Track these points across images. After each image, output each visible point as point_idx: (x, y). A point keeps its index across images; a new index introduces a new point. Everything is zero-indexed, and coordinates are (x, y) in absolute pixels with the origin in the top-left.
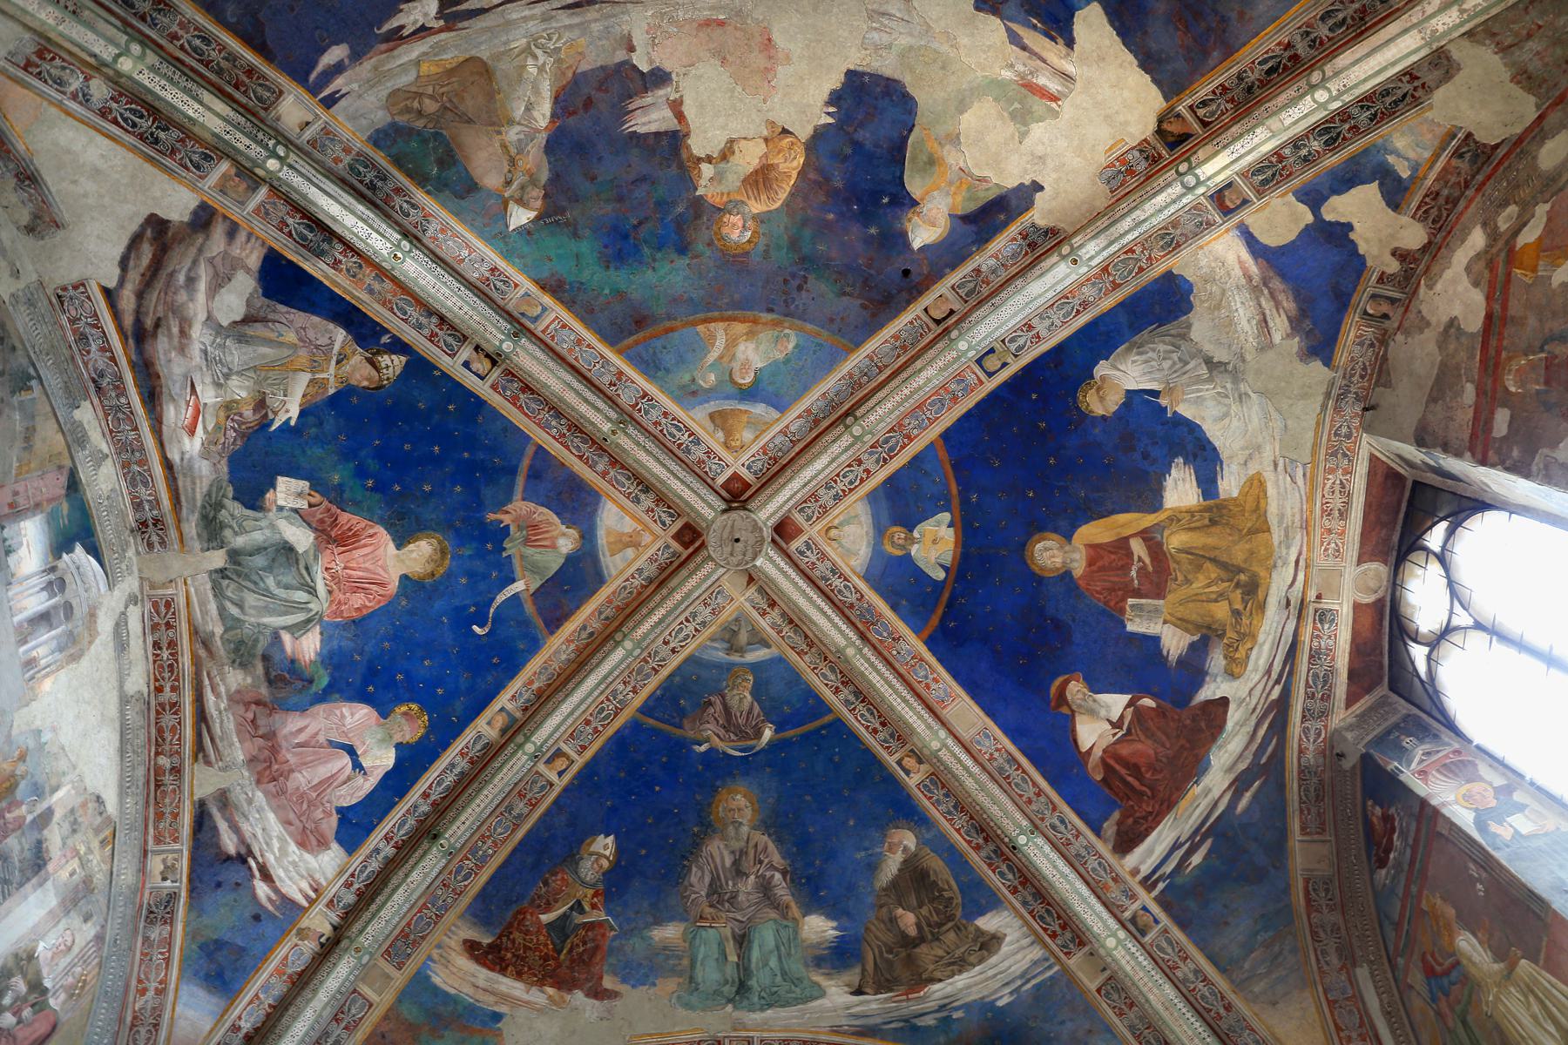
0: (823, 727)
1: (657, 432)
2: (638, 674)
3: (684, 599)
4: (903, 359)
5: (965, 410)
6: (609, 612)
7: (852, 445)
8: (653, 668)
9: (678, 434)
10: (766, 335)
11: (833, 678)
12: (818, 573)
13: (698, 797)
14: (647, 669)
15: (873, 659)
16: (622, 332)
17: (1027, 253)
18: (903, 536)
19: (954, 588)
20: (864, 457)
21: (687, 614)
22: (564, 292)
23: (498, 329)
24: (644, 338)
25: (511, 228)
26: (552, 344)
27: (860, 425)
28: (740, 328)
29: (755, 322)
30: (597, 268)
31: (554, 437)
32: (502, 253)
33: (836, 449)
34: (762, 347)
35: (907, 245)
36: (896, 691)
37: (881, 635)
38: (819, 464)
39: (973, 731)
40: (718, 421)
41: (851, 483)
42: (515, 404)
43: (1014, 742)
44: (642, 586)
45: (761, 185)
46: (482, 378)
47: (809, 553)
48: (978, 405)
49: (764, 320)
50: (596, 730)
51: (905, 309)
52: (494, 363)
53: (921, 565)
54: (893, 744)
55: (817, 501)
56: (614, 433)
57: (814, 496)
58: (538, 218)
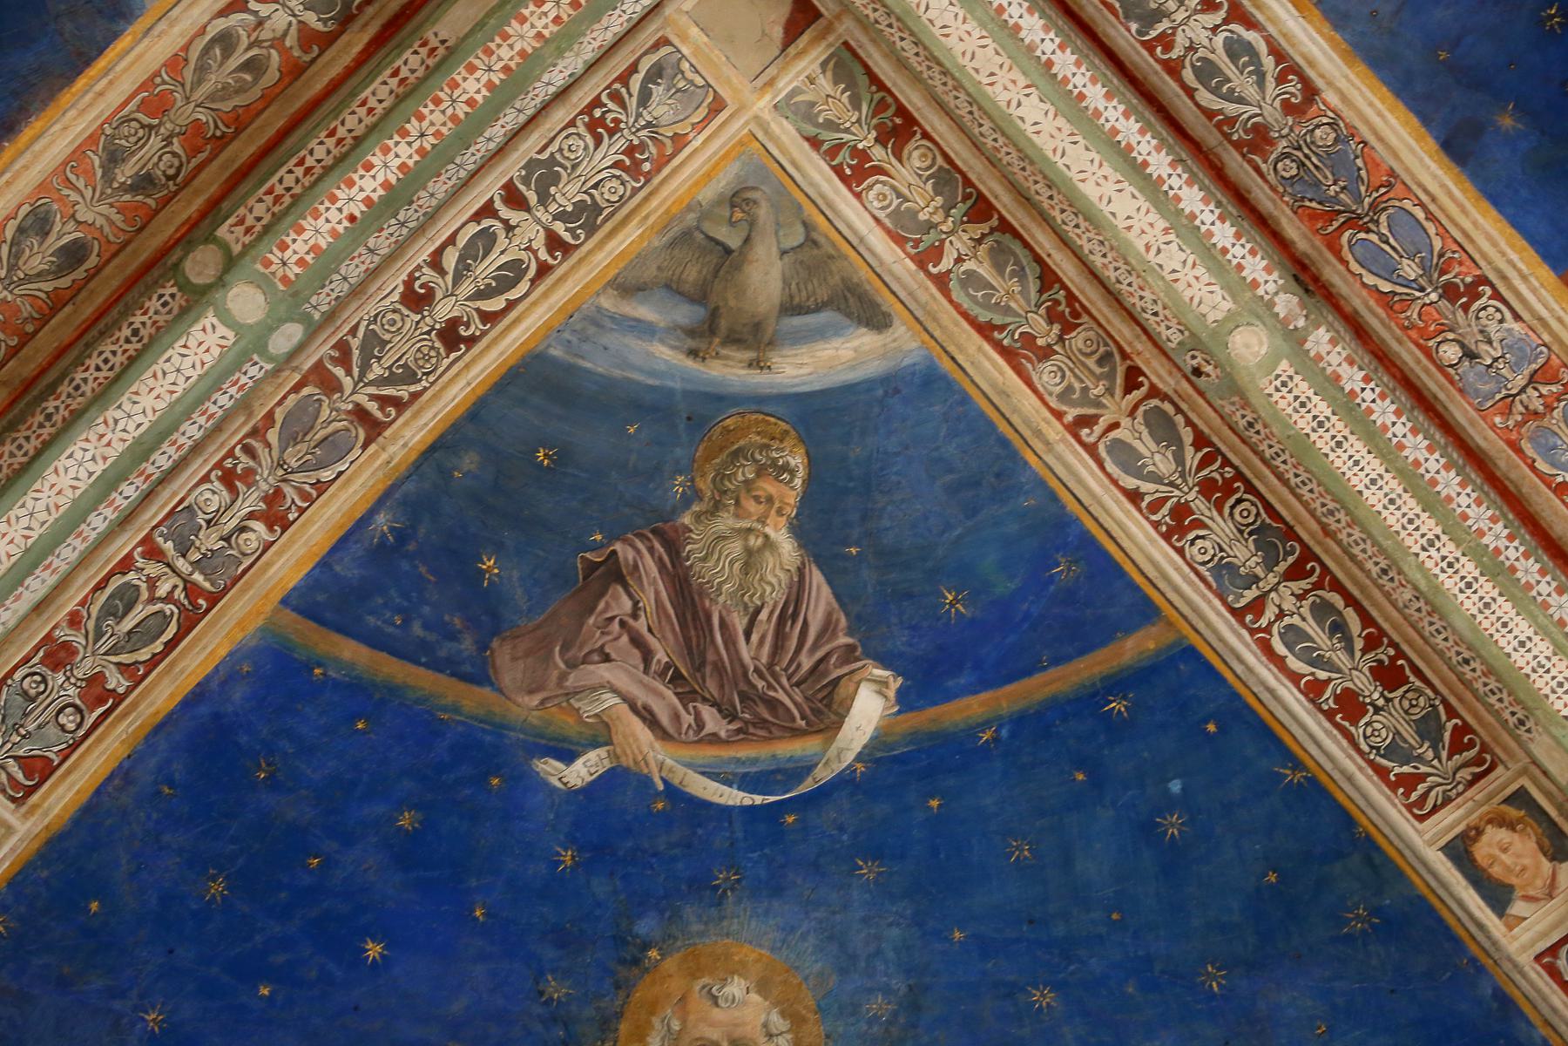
0: (1116, 684)
2: (289, 439)
3: (501, 96)
6: (151, 154)
8: (360, 414)
11: (1163, 464)
13: (556, 989)
14: (331, 416)
15: (1352, 378)
21: (511, 168)
36: (1454, 526)
44: (308, 37)
50: (96, 691)
54: (1436, 766)
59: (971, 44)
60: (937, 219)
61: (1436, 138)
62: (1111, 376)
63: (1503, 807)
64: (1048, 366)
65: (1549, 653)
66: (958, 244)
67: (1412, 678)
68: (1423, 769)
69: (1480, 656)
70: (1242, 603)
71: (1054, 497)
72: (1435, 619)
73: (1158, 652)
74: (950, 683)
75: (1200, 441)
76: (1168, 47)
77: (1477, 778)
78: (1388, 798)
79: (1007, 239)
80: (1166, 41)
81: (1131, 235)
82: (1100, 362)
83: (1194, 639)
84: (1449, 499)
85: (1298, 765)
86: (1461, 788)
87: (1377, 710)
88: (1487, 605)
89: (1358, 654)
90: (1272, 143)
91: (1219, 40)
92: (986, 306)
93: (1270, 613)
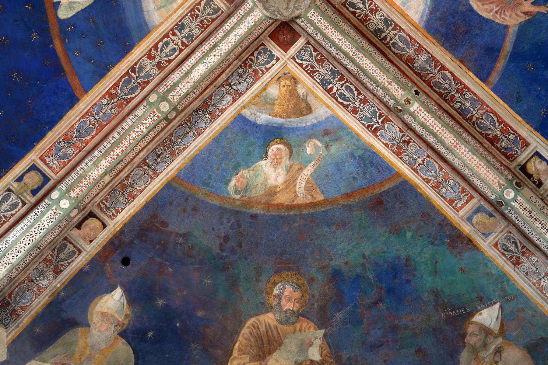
1: (364, 92)
4: (123, 175)
5: (56, 128)
7: (169, 91)
9: (344, 91)
10: (258, 192)
16: (395, 194)
17: (10, 295)
22: (450, 236)
23: (515, 212)
24: (373, 188)
25: (497, 306)
26: (464, 184)
28: (282, 199)
29: (268, 205)
30: (418, 259)
31: (469, 89)
32: (508, 281)
33: (186, 87)
34: (261, 180)
35: (127, 292)
40: (303, 105)
41: (167, 44)
42: (506, 125)
45: (265, 340)
46: (537, 154)
48: (42, 135)
49: (260, 207)
51: (125, 226)
52: (523, 168)
55: (201, 22)
56: (408, 101)
58: (471, 314)
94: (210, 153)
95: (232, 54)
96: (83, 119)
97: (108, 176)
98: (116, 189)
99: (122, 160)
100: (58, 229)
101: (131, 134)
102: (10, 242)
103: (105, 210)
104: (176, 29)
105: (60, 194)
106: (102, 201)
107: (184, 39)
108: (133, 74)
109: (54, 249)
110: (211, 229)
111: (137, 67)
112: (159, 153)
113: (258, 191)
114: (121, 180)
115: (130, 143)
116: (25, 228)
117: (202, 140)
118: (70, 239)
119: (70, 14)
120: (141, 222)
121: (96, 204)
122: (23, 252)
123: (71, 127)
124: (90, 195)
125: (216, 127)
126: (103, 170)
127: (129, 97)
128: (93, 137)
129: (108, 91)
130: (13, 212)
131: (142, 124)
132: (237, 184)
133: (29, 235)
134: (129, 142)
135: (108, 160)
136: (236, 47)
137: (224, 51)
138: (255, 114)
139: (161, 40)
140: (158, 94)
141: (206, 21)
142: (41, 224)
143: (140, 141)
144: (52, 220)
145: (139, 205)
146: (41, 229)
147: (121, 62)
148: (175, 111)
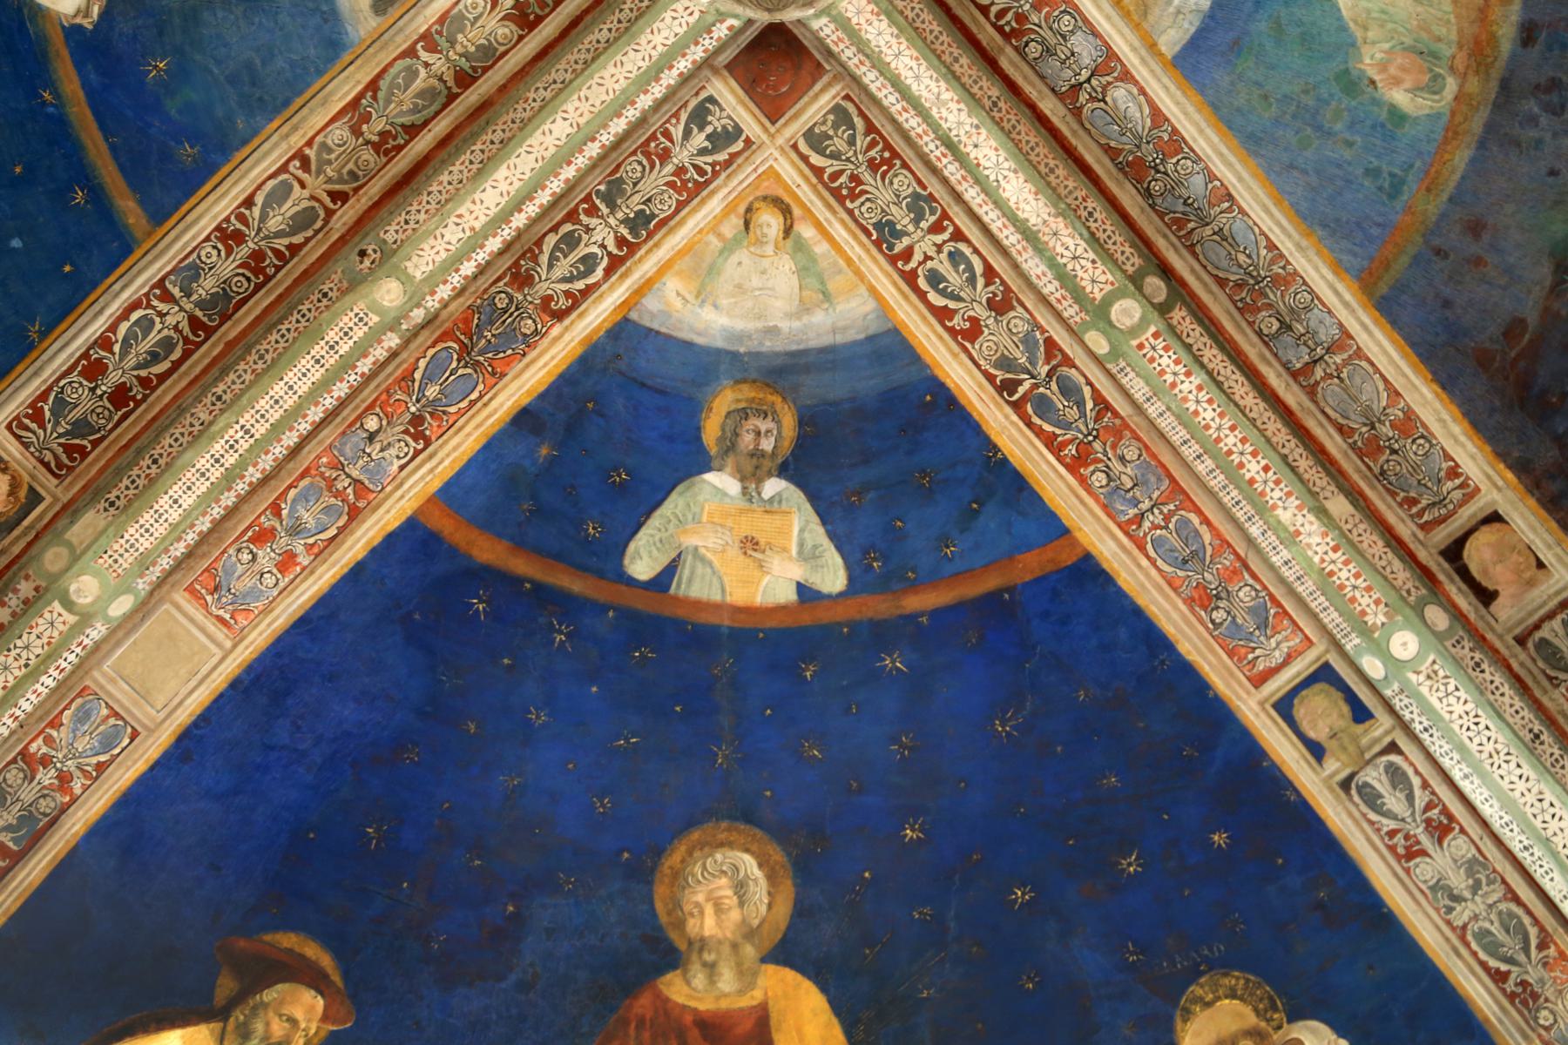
0: (97, 195)
4: (1334, 444)
5: (1169, 629)
7: (1078, 295)
11: (275, 223)
12: (632, 169)
18: (767, 445)
19: (604, 608)
20: (1017, 321)
27: (1143, 323)
33: (1068, 243)
36: (261, 446)
37: (428, 378)
38: (1019, 191)
39: (121, 694)
41: (935, 279)
43: (100, 830)
47: (699, 139)
51: (1502, 455)
53: (674, 505)
54: (53, 435)
55: (873, 166)
57: (887, 161)
59: (609, 83)
60: (459, 48)
61: (530, 404)
62: (341, 181)
63: (25, 487)
64: (346, 133)
65: (170, 520)
66: (438, 63)
67: (120, 413)
68: (49, 427)
69: (163, 472)
70: (169, 286)
71: (245, 142)
72: (187, 438)
73: (126, 226)
74: (90, 67)
75: (294, 249)
76: (588, 213)
77: (46, 465)
78: (23, 403)
79: (442, 99)
80: (593, 211)
81: (468, 204)
82: (351, 173)
83: (138, 253)
84: (280, 440)
85: (44, 334)
86: (37, 454)
87: (93, 390)
88: (203, 475)
89: (135, 373)
90: (520, 289)
91: (595, 249)
92: (392, 85)
93: (163, 307)
94: (1292, 166)
95: (975, 90)
96: (1149, 547)
97: (1329, 505)
98: (1377, 470)
99: (1284, 458)
100: (1482, 671)
101: (1203, 423)
102: (1507, 818)
103: (1444, 511)
104: (891, 248)
105: (1373, 654)
106: (1412, 516)
107: (924, 225)
108: (1021, 390)
109: (1550, 679)
110: (1550, 180)
111: (1000, 375)
112: (1276, 325)
113: (1439, 14)
114: (1350, 452)
115: (1233, 428)
116: (1467, 770)
117: (1249, 188)
118: (1523, 626)
119: (834, 559)
120: (1497, 403)
121: (1421, 535)
122: (1542, 786)
123: (1170, 584)
124: (1384, 563)
125: (1208, 140)
126: (1311, 517)
127: (1090, 405)
128: (1206, 521)
129: (1067, 466)
130: (1416, 782)
131: (1173, 385)
132: (1407, 85)
133: (1490, 761)
134: (1227, 432)
135: (1280, 499)
136: (953, 77)
137: (964, 116)
138: (1179, 12)
139: (922, 295)
140: (1086, 326)
141: (872, 153)
142: (1460, 722)
143: (1229, 397)
144: (1451, 688)
145: (1438, 405)
146: (1477, 724)
147: (981, 423)
148: (1143, 278)
